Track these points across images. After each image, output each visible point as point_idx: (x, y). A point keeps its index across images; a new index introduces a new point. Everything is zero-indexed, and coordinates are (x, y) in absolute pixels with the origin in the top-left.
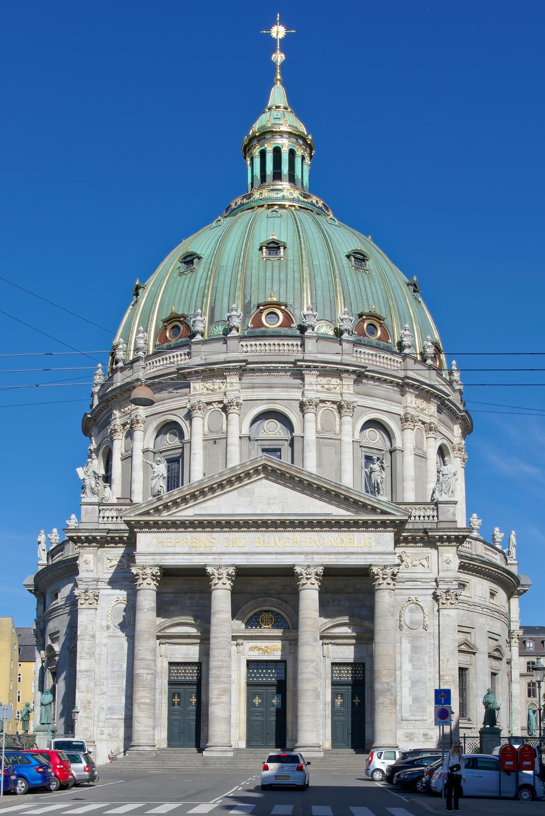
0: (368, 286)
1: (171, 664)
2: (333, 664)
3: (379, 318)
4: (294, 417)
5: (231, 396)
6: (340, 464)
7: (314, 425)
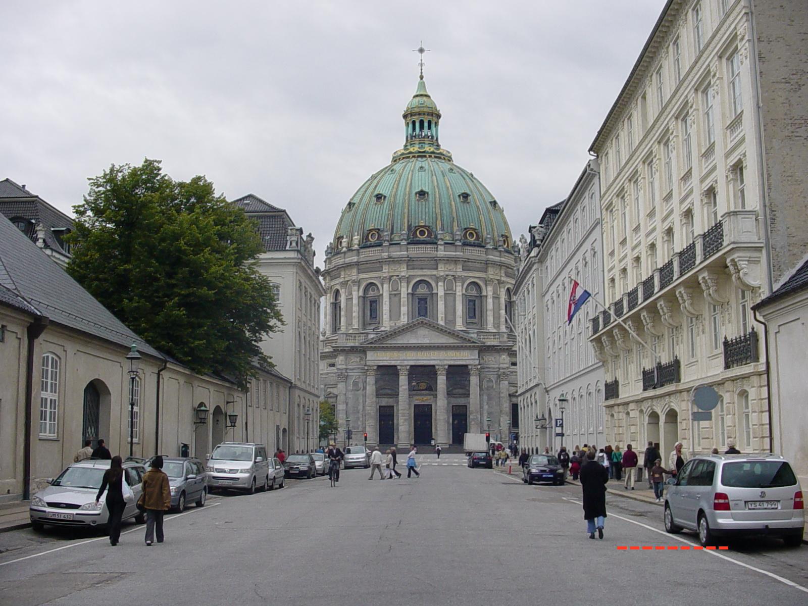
0: (469, 211)
1: (380, 407)
2: (453, 406)
3: (474, 230)
4: (434, 284)
5: (403, 274)
6: (455, 305)
7: (443, 288)
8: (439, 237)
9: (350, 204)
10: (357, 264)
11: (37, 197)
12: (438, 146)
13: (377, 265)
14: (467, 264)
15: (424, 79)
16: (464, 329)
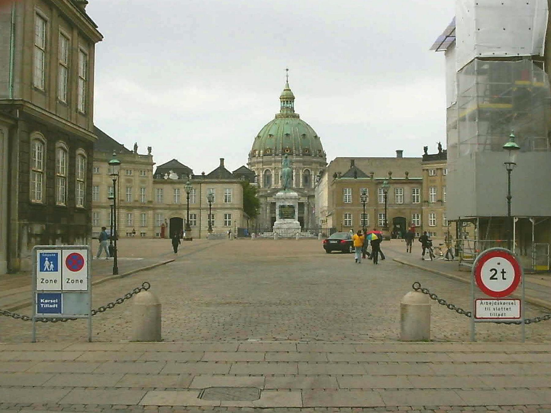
3: (308, 149)
8: (294, 152)
9: (258, 137)
10: (262, 162)
11: (187, 167)
12: (294, 111)
13: (270, 163)
14: (304, 163)
15: (288, 82)
16: (303, 187)
